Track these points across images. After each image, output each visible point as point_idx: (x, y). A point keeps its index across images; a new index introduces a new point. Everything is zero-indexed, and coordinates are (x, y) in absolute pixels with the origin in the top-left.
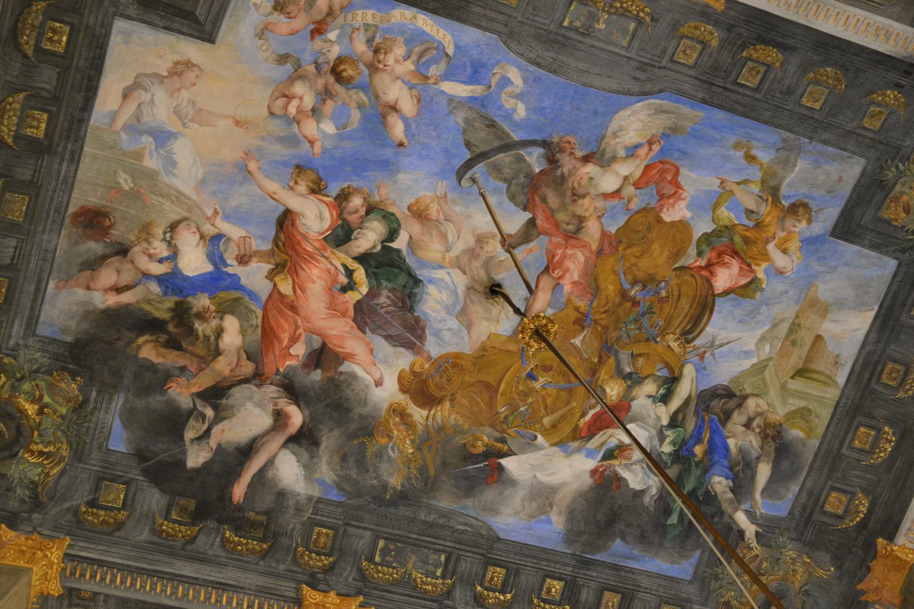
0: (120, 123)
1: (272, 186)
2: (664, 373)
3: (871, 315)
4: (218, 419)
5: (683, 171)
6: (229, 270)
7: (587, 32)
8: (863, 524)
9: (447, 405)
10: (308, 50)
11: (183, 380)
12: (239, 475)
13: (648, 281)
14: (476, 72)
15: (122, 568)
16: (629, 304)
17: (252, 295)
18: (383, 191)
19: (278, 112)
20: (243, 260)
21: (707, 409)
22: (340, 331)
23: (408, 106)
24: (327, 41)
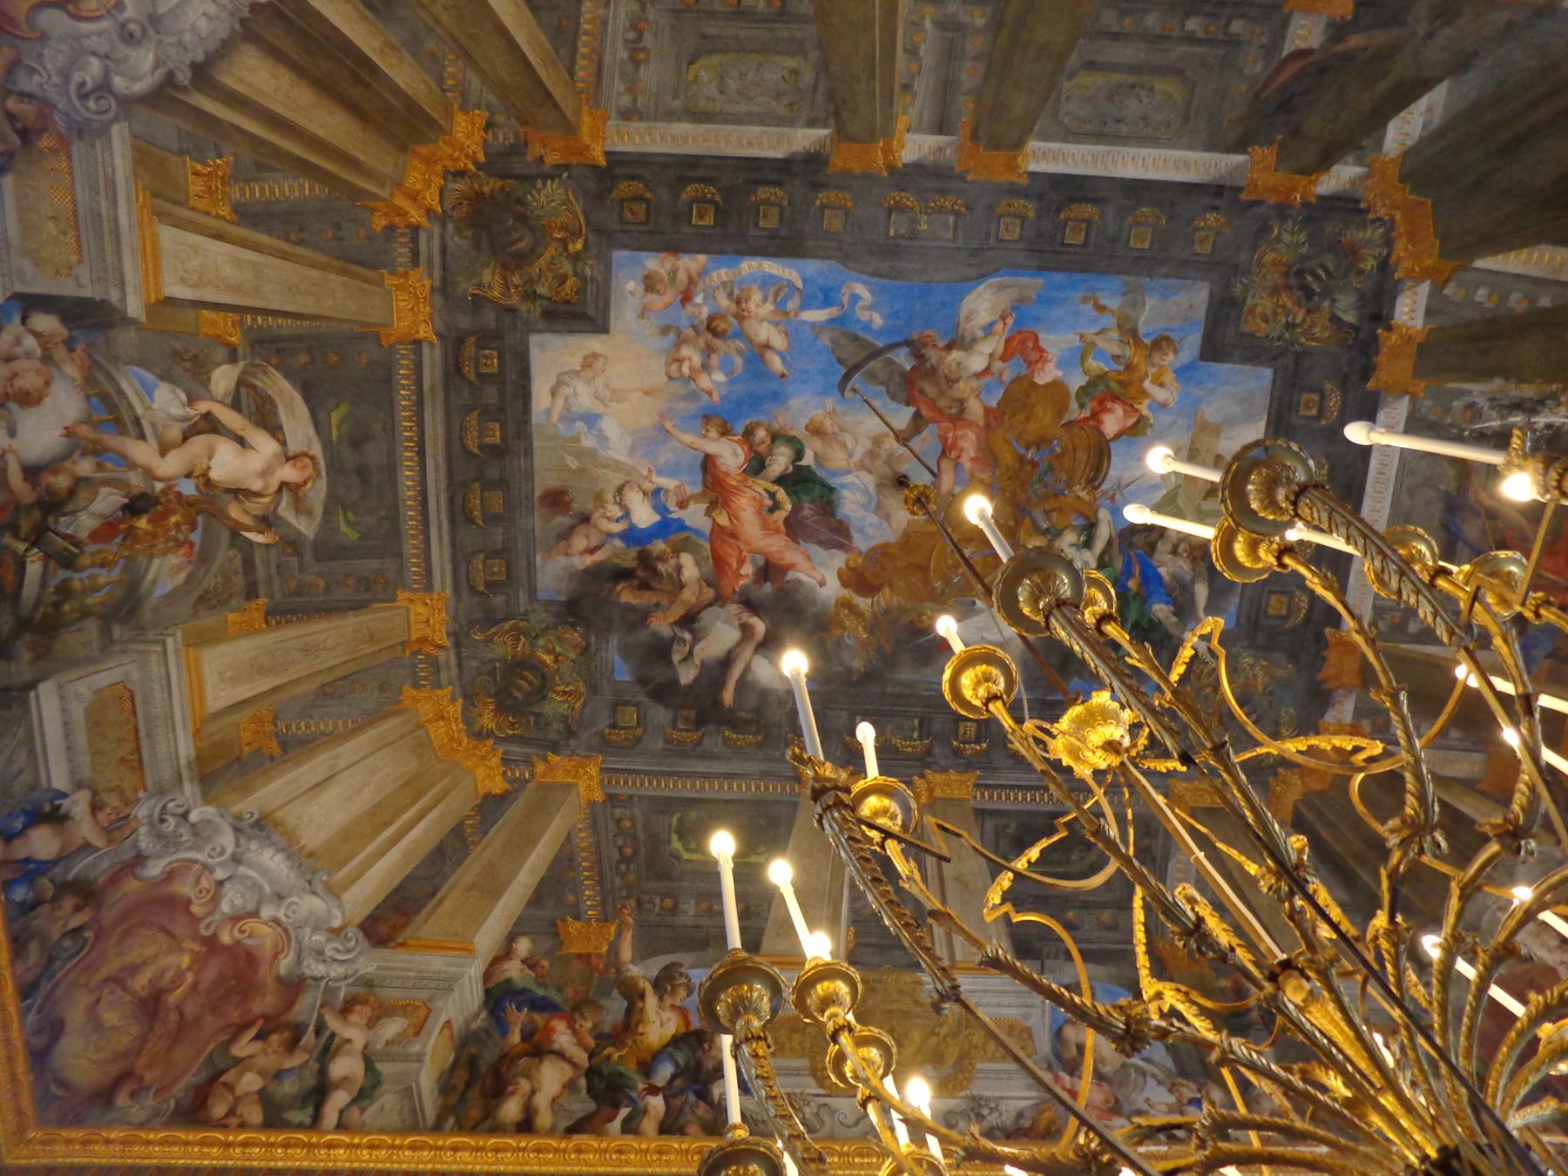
0: (555, 417)
1: (689, 438)
2: (1079, 522)
3: (1262, 425)
4: (696, 640)
5: (1042, 336)
6: (673, 516)
7: (913, 235)
8: (1308, 620)
9: (887, 590)
10: (683, 317)
11: (659, 614)
12: (724, 683)
13: (1042, 442)
14: (826, 296)
15: (647, 773)
16: (1028, 468)
17: (698, 532)
18: (780, 419)
19: (675, 375)
20: (682, 505)
21: (1131, 546)
22: (777, 545)
23: (779, 341)
24: (696, 305)
